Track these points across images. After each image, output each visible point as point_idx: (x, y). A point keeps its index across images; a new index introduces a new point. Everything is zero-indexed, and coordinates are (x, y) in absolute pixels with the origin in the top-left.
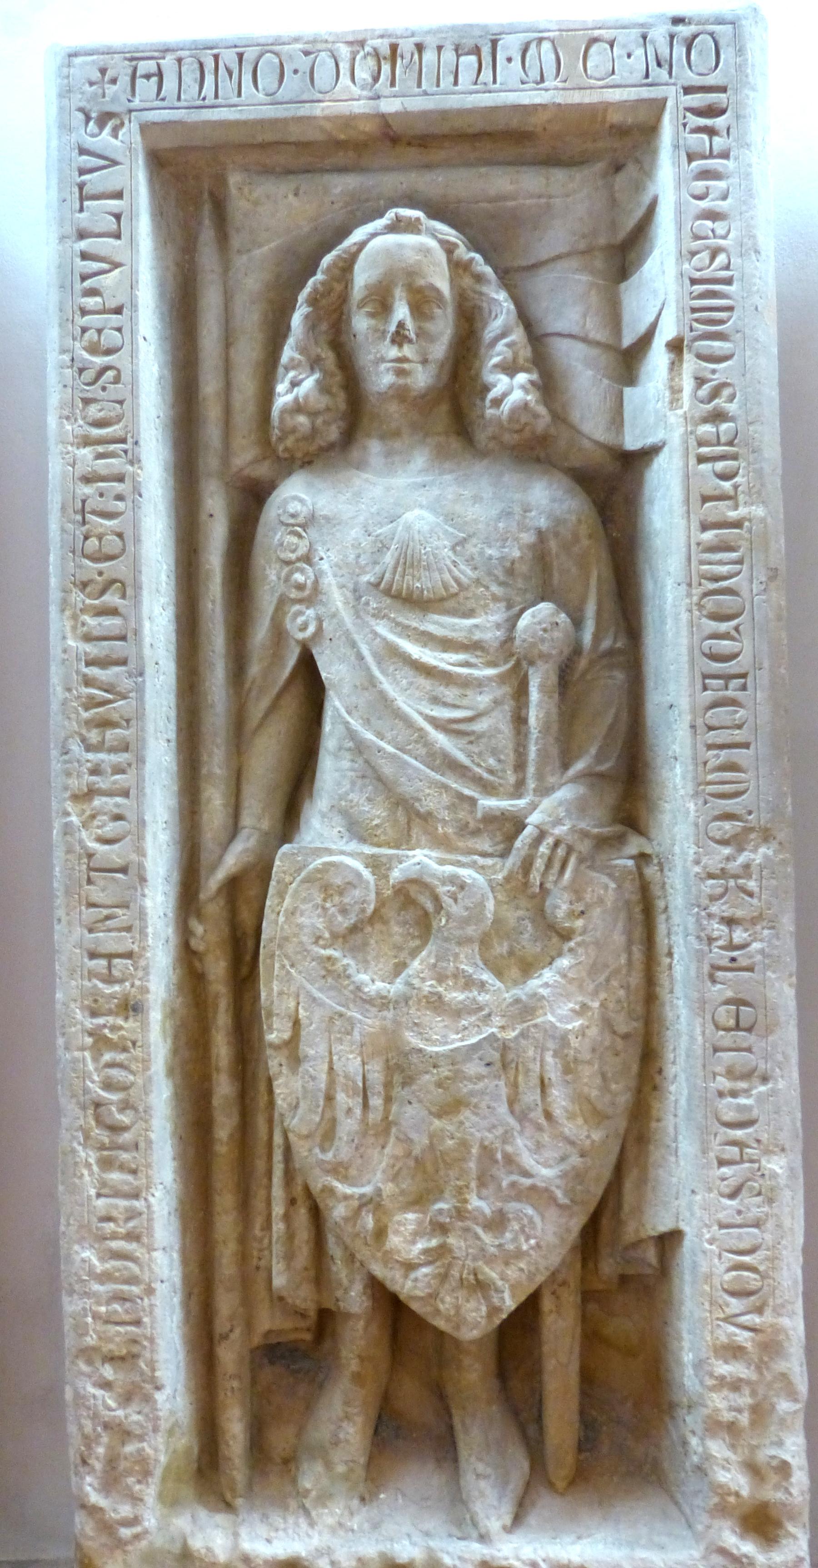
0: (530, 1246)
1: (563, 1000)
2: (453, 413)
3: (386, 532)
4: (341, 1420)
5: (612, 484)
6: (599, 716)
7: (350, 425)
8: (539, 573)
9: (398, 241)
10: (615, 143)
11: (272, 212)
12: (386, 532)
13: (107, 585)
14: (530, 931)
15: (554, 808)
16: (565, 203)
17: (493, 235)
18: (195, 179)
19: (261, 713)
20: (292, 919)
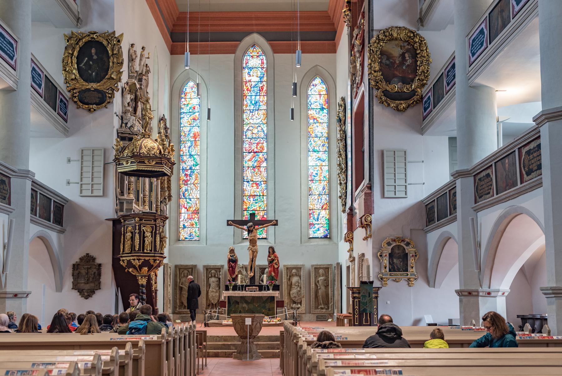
0: (216, 301)
1: (217, 294)
2: (215, 276)
3: (212, 280)
4: (210, 307)
5: (220, 279)
6: (219, 286)
7: (212, 277)
8: (217, 281)
9: (213, 271)
10: (220, 269)
11: (209, 270)
12: (212, 280)
13: (204, 281)
14: (216, 292)
15: (217, 288)
16: (218, 270)
17: (216, 271)
18: (207, 269)
19: (208, 285)
20: (209, 292)
